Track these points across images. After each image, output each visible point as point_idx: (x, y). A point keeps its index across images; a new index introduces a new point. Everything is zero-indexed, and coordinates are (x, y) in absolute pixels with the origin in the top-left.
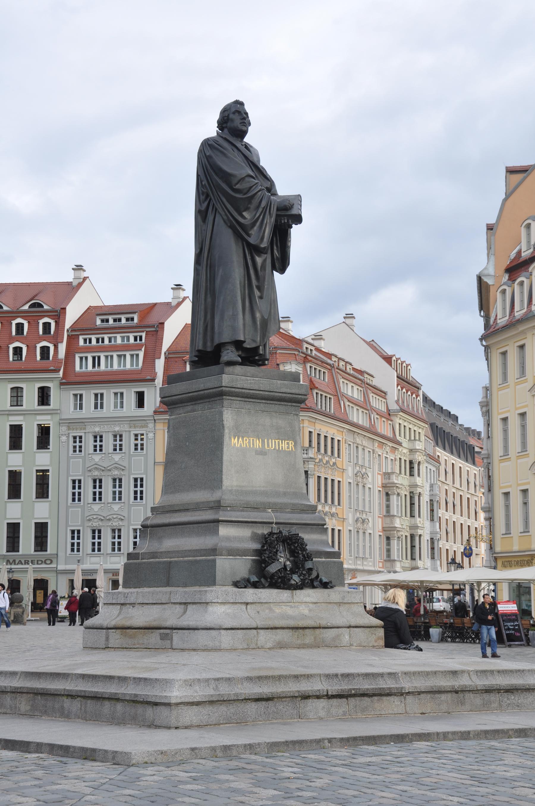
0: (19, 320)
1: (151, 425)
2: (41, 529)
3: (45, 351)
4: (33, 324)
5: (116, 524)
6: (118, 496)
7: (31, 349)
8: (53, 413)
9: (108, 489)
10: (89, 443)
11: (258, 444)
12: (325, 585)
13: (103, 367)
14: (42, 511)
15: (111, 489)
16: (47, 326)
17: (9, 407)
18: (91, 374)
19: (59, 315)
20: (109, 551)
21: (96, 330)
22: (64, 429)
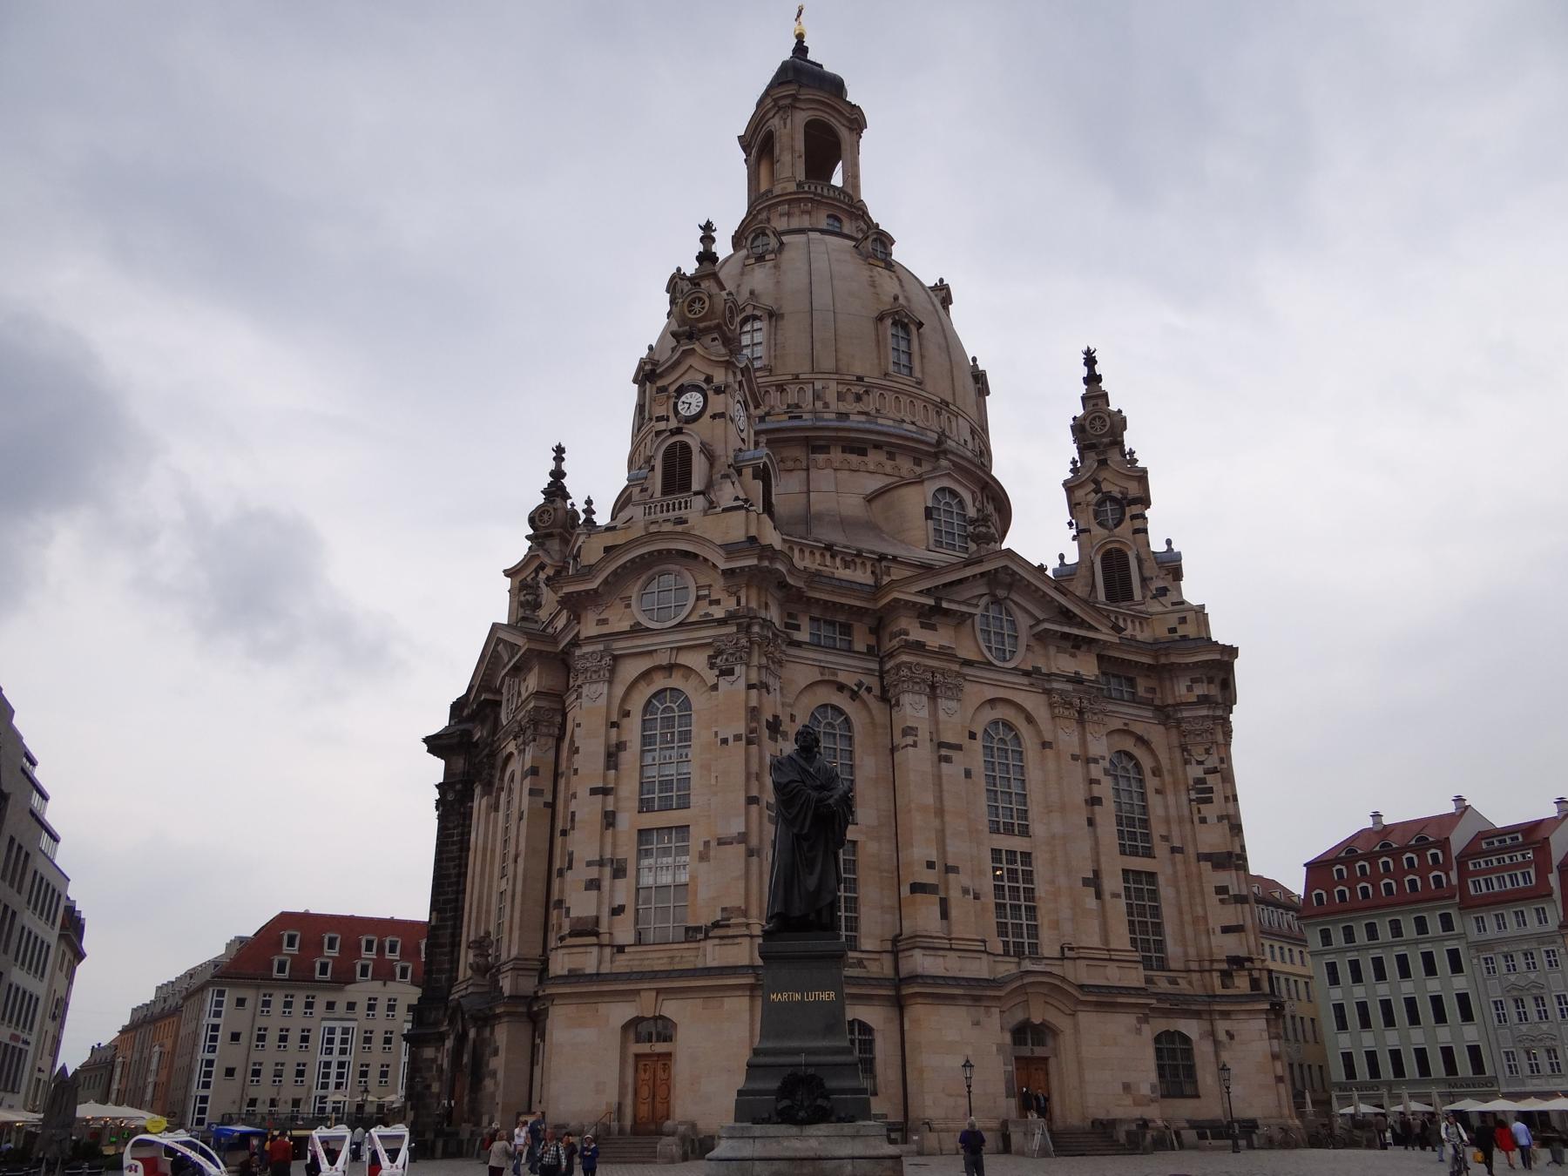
0: (1409, 855)
1: (1560, 940)
2: (1474, 1052)
3: (1438, 879)
4: (1422, 857)
5: (1549, 1043)
6: (1542, 1015)
7: (1400, 884)
8: (1459, 937)
9: (1531, 1008)
10: (1501, 964)
11: (798, 997)
12: (840, 1120)
13: (1522, 884)
14: (1471, 1033)
15: (1534, 1008)
16: (1435, 856)
17: (1415, 936)
18: (1507, 892)
19: (1444, 844)
20: (1549, 1072)
21: (1483, 854)
22: (1472, 951)
